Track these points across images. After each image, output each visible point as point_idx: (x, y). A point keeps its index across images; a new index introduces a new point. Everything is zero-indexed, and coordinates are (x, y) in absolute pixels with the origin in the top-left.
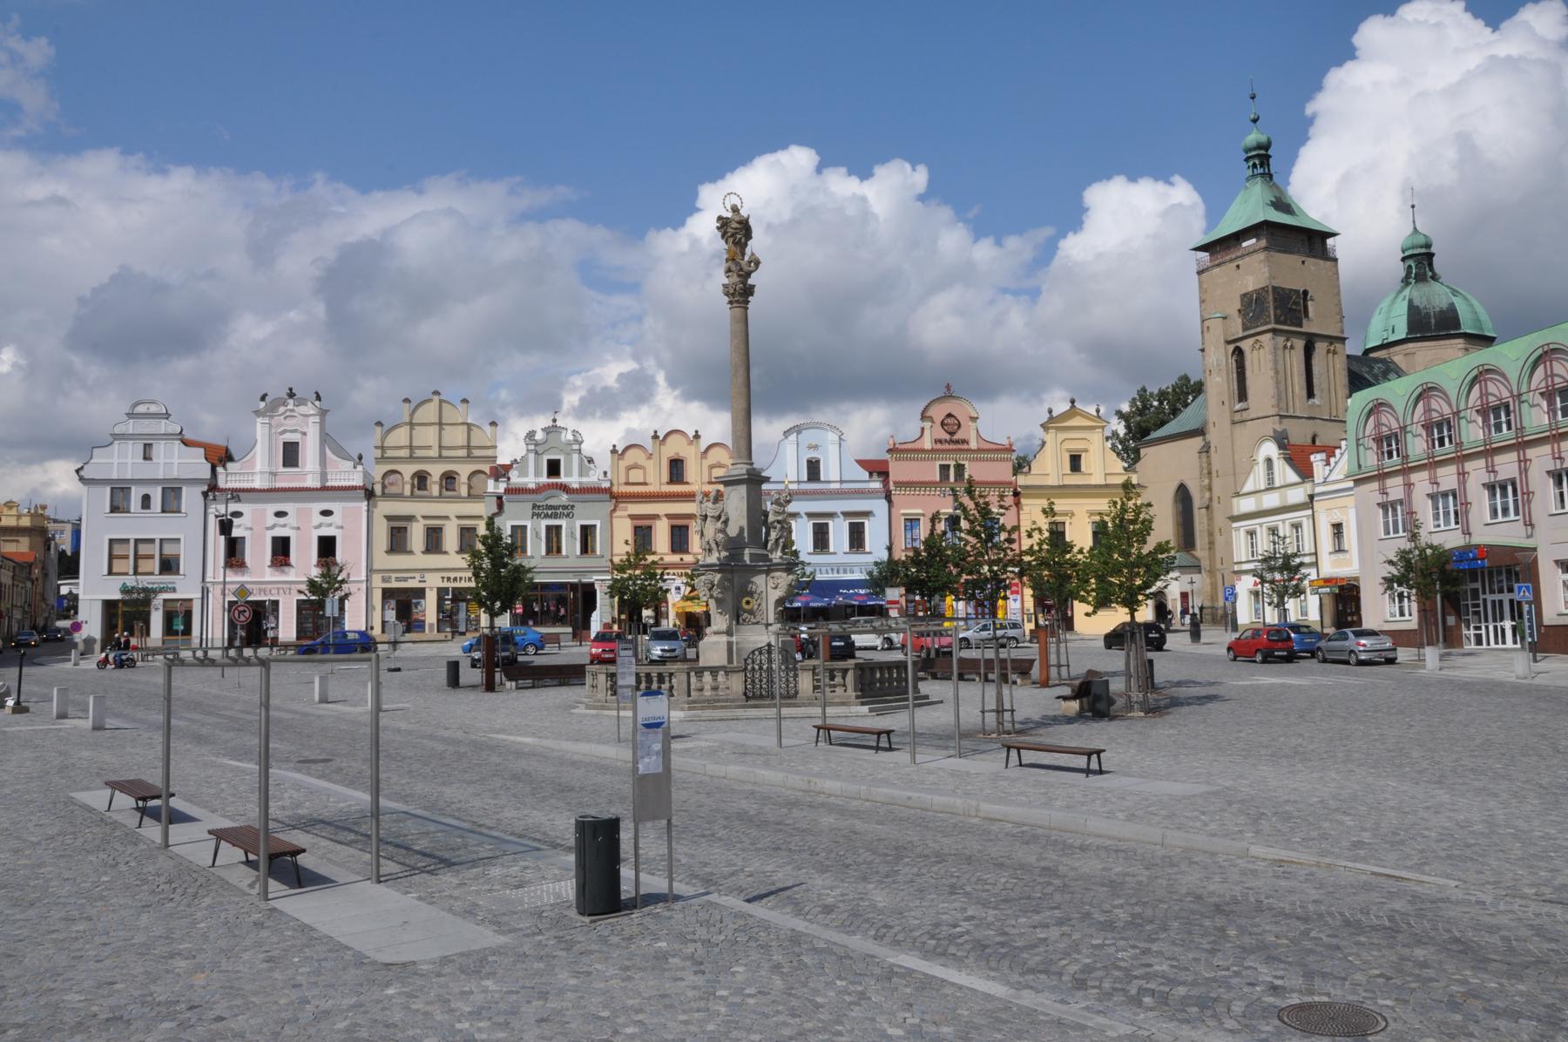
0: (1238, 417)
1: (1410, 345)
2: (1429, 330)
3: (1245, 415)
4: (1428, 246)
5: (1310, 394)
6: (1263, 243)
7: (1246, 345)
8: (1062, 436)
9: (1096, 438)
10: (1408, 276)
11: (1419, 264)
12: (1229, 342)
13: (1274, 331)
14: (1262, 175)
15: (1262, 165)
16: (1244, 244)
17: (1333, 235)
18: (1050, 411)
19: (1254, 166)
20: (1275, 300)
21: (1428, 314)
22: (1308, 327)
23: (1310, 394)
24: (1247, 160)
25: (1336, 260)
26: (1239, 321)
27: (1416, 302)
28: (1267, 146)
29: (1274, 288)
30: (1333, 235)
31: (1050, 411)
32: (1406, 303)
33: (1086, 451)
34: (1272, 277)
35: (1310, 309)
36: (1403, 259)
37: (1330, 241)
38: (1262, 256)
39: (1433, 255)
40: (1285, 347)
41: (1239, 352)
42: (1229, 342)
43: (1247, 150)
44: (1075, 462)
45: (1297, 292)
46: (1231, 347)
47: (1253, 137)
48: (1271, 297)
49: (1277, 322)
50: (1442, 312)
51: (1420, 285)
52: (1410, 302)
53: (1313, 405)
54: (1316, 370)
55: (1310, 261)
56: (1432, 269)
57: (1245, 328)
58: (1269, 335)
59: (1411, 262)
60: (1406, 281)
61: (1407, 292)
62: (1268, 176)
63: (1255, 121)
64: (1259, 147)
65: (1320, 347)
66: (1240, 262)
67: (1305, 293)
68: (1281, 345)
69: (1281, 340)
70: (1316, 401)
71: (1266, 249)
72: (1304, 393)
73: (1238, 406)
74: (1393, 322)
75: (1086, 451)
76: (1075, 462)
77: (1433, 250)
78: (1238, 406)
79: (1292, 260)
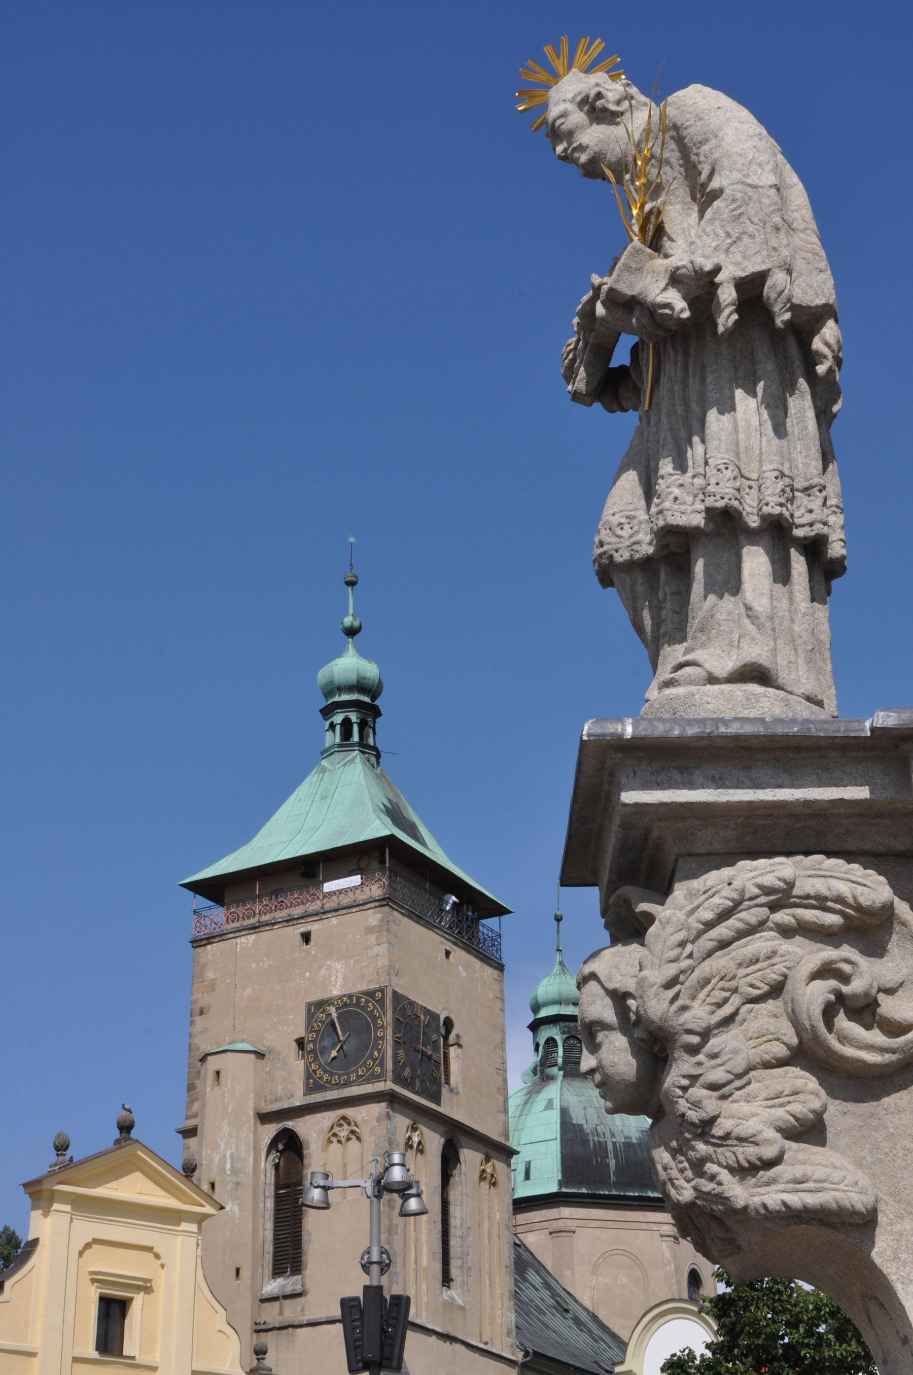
0: (271, 1315)
1: (566, 1211)
2: (605, 1183)
3: (291, 1311)
5: (447, 1280)
6: (376, 890)
7: (311, 1129)
8: (90, 1228)
9: (180, 1248)
10: (546, 1062)
11: (571, 1038)
12: (265, 1118)
13: (391, 1098)
14: (363, 745)
15: (363, 725)
16: (329, 886)
17: (500, 911)
18: (61, 1147)
19: (347, 723)
20: (397, 1023)
21: (602, 1146)
22: (449, 1108)
23: (447, 1280)
24: (327, 712)
25: (500, 968)
26: (298, 1066)
27: (577, 1117)
28: (370, 689)
29: (394, 992)
30: (500, 911)
31: (61, 1147)
32: (554, 1116)
33: (146, 1287)
34: (392, 970)
35: (455, 1066)
37: (491, 922)
38: (373, 917)
40: (408, 1145)
41: (289, 1147)
42: (265, 1118)
43: (331, 689)
44: (113, 1312)
45: (435, 1017)
46: (270, 1131)
47: (349, 664)
48: (389, 1017)
49: (398, 1079)
50: (628, 1145)
52: (565, 1113)
53: (450, 1305)
54: (455, 1212)
55: (459, 954)
57: (312, 1086)
58: (379, 1108)
59: (554, 1032)
60: (542, 1073)
61: (553, 1091)
62: (372, 753)
63: (351, 632)
64: (360, 686)
65: (470, 1158)
66: (314, 927)
67: (449, 1024)
68: (401, 1138)
69: (402, 1122)
70: (454, 1294)
71: (385, 901)
72: (438, 1266)
73: (273, 1286)
75: (146, 1287)
76: (113, 1312)
78: (273, 1286)
79: (427, 942)
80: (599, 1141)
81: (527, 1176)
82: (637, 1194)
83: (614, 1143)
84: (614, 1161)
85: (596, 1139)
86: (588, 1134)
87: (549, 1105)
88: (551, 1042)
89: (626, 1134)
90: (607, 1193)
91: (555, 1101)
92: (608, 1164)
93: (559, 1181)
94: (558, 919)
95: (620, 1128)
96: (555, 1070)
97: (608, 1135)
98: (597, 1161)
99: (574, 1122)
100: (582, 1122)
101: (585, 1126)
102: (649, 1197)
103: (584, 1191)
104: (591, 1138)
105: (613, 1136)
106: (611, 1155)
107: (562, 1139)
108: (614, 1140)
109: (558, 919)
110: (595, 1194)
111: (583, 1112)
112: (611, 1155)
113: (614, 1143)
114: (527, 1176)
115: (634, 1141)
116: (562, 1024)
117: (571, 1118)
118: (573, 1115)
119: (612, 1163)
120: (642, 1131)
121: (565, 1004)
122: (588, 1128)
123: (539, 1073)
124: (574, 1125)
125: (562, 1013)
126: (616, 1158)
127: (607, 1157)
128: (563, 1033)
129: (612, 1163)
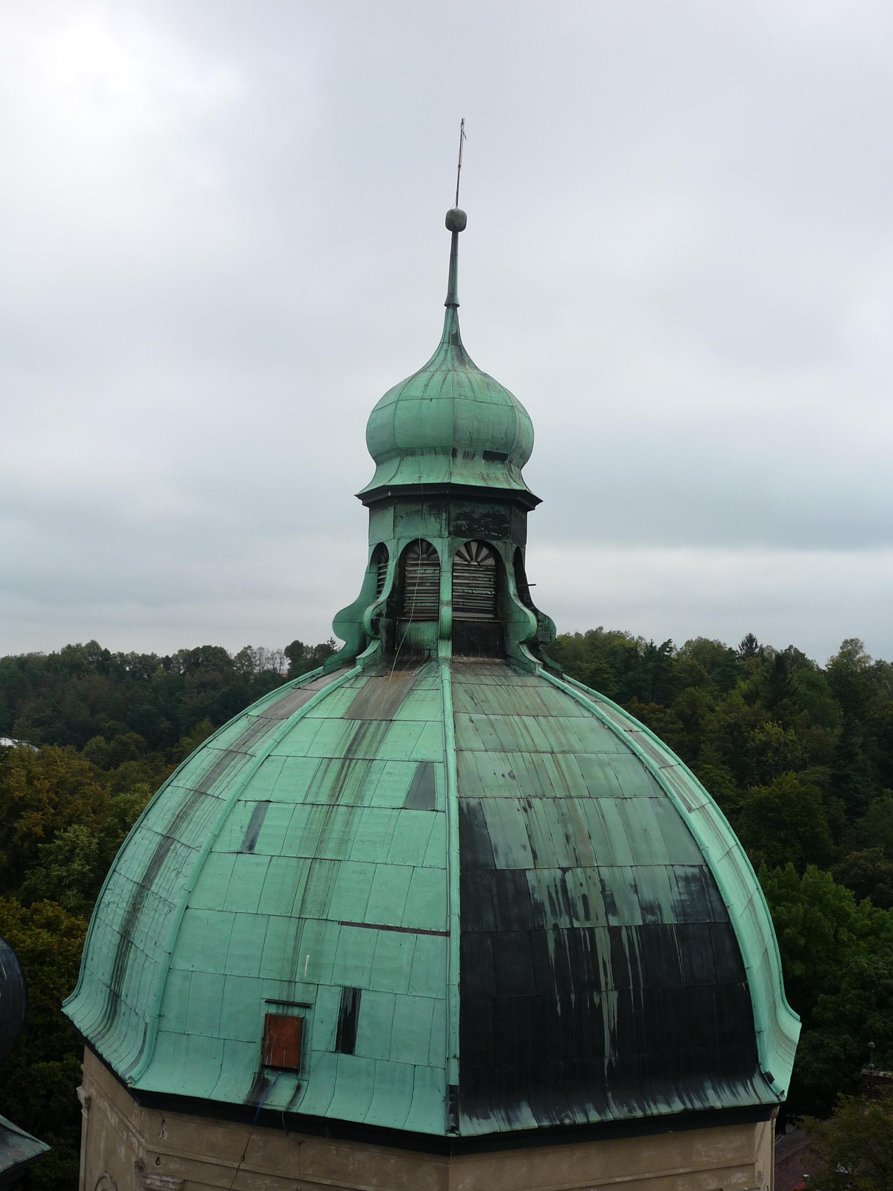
4: (508, 450)
21: (579, 944)
27: (510, 850)
32: (436, 842)
36: (375, 500)
39: (529, 501)
50: (653, 934)
51: (492, 687)
56: (529, 604)
74: (348, 959)
77: (533, 477)
80: (572, 930)
81: (346, 1039)
82: (678, 1106)
83: (615, 932)
84: (614, 996)
85: (564, 922)
86: (539, 908)
87: (422, 793)
88: (419, 550)
89: (647, 895)
90: (594, 1117)
91: (439, 769)
92: (597, 1011)
93: (451, 1089)
94: (456, 223)
95: (629, 874)
96: (426, 632)
97: (597, 904)
98: (566, 1002)
99: (501, 863)
100: (523, 860)
101: (530, 876)
102: (712, 1109)
103: (527, 1120)
104: (550, 921)
105: (611, 907)
106: (606, 979)
107: (464, 935)
108: (614, 922)
109: (456, 223)
110: (563, 1126)
111: (521, 817)
112: (606, 979)
113: (615, 932)
114: (346, 1039)
115: (669, 918)
116: (455, 511)
117: (492, 851)
118: (496, 836)
119: (609, 1002)
120: (687, 879)
121: (466, 455)
122: (541, 880)
123: (383, 634)
124: (500, 874)
125: (457, 480)
126: (621, 985)
127: (596, 985)
128: (456, 532)
129: (609, 1002)
